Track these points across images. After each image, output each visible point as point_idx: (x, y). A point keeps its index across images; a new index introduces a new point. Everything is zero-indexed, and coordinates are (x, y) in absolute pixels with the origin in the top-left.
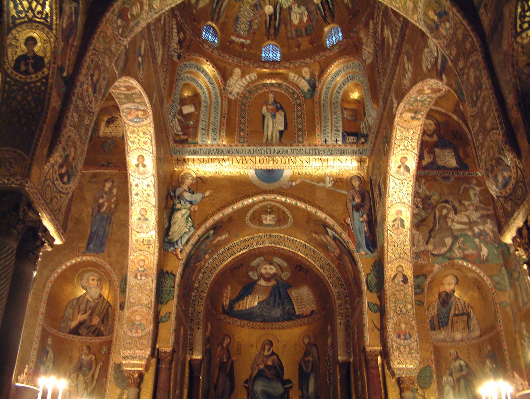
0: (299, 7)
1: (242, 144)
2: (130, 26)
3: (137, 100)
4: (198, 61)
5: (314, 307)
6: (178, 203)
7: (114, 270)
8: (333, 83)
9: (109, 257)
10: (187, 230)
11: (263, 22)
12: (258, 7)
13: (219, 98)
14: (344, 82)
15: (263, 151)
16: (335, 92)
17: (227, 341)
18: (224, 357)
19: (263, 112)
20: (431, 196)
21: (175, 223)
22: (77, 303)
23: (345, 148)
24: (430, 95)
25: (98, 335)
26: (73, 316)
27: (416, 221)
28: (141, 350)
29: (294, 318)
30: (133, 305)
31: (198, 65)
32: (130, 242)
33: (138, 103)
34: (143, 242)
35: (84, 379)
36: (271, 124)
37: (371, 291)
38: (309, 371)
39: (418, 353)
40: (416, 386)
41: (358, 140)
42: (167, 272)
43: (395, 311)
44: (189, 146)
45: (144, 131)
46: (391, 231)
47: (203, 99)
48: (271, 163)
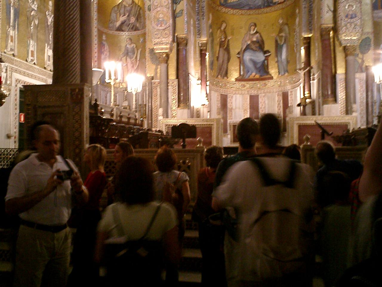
17: (224, 25)
18: (223, 37)
22: (118, 8)
25: (135, 30)
26: (116, 18)
28: (166, 38)
29: (271, 5)
30: (156, 7)
35: (131, 60)
38: (282, 44)
40: (358, 51)
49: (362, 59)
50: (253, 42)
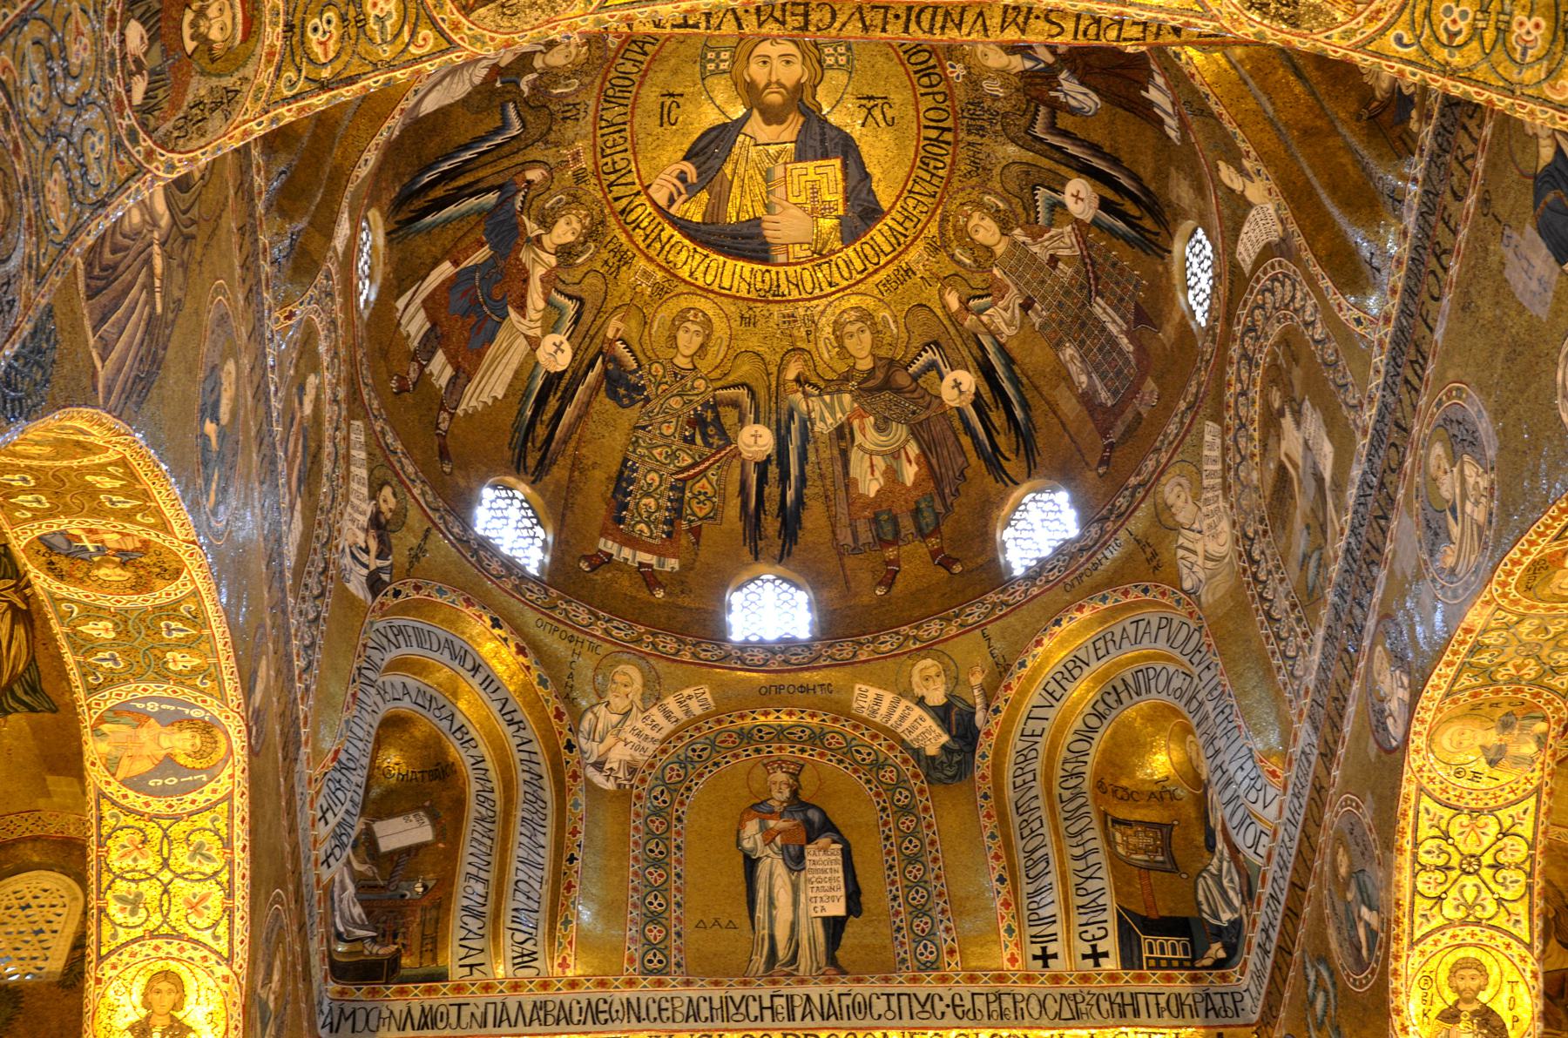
0: (879, 429)
1: (657, 974)
2: (190, 98)
3: (179, 661)
11: (733, 488)
12: (711, 430)
13: (547, 782)
14: (1101, 707)
15: (754, 1009)
16: (1063, 753)
19: (747, 844)
33: (182, 678)
36: (783, 897)
41: (1195, 952)
44: (402, 992)
45: (195, 838)
47: (473, 787)
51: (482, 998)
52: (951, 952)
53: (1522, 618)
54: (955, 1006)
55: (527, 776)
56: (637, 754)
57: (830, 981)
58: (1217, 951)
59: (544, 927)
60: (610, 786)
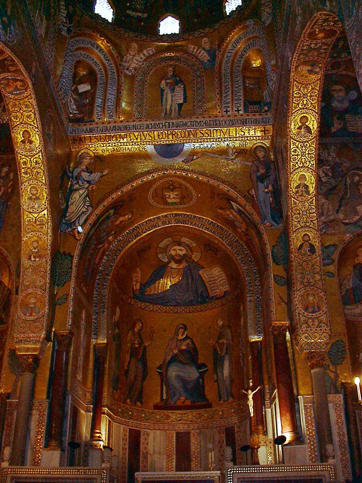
3: (13, 69)
4: (90, 36)
5: (226, 288)
6: (76, 184)
7: (10, 254)
8: (234, 51)
9: (5, 241)
10: (85, 210)
13: (115, 74)
15: (161, 126)
16: (236, 61)
19: (162, 86)
20: (341, 163)
21: (72, 204)
23: (247, 117)
24: (324, 41)
27: (324, 189)
30: (28, 287)
31: (92, 42)
32: (22, 223)
33: (13, 72)
34: (35, 222)
36: (169, 98)
37: (277, 264)
39: (327, 325)
40: (327, 362)
42: (64, 253)
43: (302, 283)
44: (85, 125)
46: (294, 198)
47: (99, 76)
48: (170, 137)
49: (336, 372)
50: (181, 351)
51: (102, 126)
52: (206, 111)
53: (311, 44)
54: (206, 123)
55: (111, 73)
56: (137, 66)
57: (178, 119)
58: (266, 108)
59: (114, 109)
60: (130, 74)
